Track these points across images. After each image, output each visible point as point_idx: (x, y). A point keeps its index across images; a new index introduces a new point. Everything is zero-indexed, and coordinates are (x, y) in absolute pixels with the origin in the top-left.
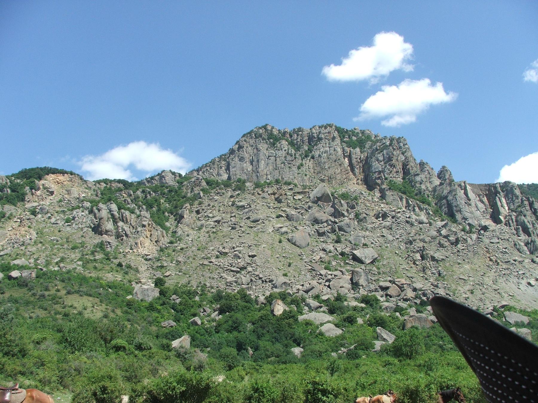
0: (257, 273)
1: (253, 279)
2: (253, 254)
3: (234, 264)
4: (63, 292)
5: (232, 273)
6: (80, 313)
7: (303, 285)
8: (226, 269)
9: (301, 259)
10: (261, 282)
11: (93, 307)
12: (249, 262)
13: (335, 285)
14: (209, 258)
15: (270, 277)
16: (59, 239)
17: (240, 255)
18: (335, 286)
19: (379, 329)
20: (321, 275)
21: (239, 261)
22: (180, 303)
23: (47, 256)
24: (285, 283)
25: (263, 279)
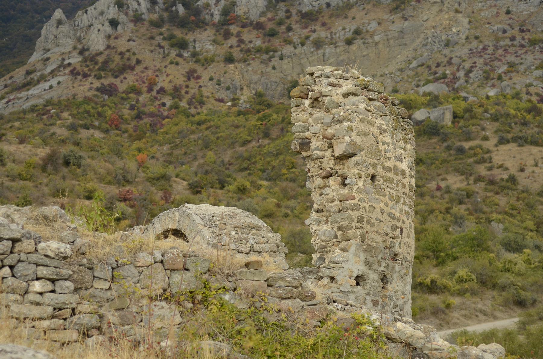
4: (494, 141)
6: (512, 179)
11: (536, 165)
16: (507, 27)
23: (486, 64)
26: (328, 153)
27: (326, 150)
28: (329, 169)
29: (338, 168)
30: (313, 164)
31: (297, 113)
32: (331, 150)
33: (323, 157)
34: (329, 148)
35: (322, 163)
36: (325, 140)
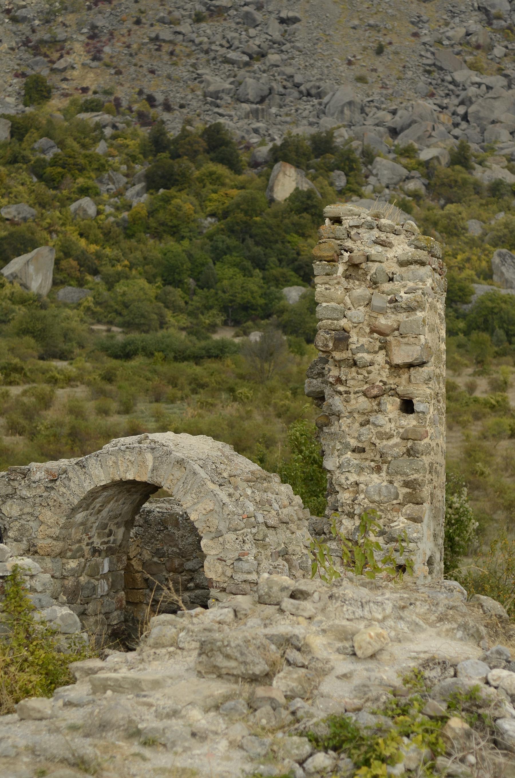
0: (289, 70)
1: (277, 87)
2: (291, 14)
3: (236, 43)
5: (227, 66)
7: (394, 113)
8: (212, 54)
9: (415, 35)
10: (296, 94)
12: (277, 36)
13: (481, 115)
14: (176, 22)
15: (322, 84)
17: (259, 16)
18: (479, 118)
19: (500, 255)
20: (453, 82)
21: (252, 32)
22: (54, 163)
24: (350, 103)
25: (302, 88)
26: (381, 357)
27: (376, 352)
28: (381, 384)
29: (391, 382)
30: (354, 374)
31: (327, 286)
32: (383, 352)
33: (372, 364)
34: (381, 348)
35: (369, 372)
36: (376, 335)
